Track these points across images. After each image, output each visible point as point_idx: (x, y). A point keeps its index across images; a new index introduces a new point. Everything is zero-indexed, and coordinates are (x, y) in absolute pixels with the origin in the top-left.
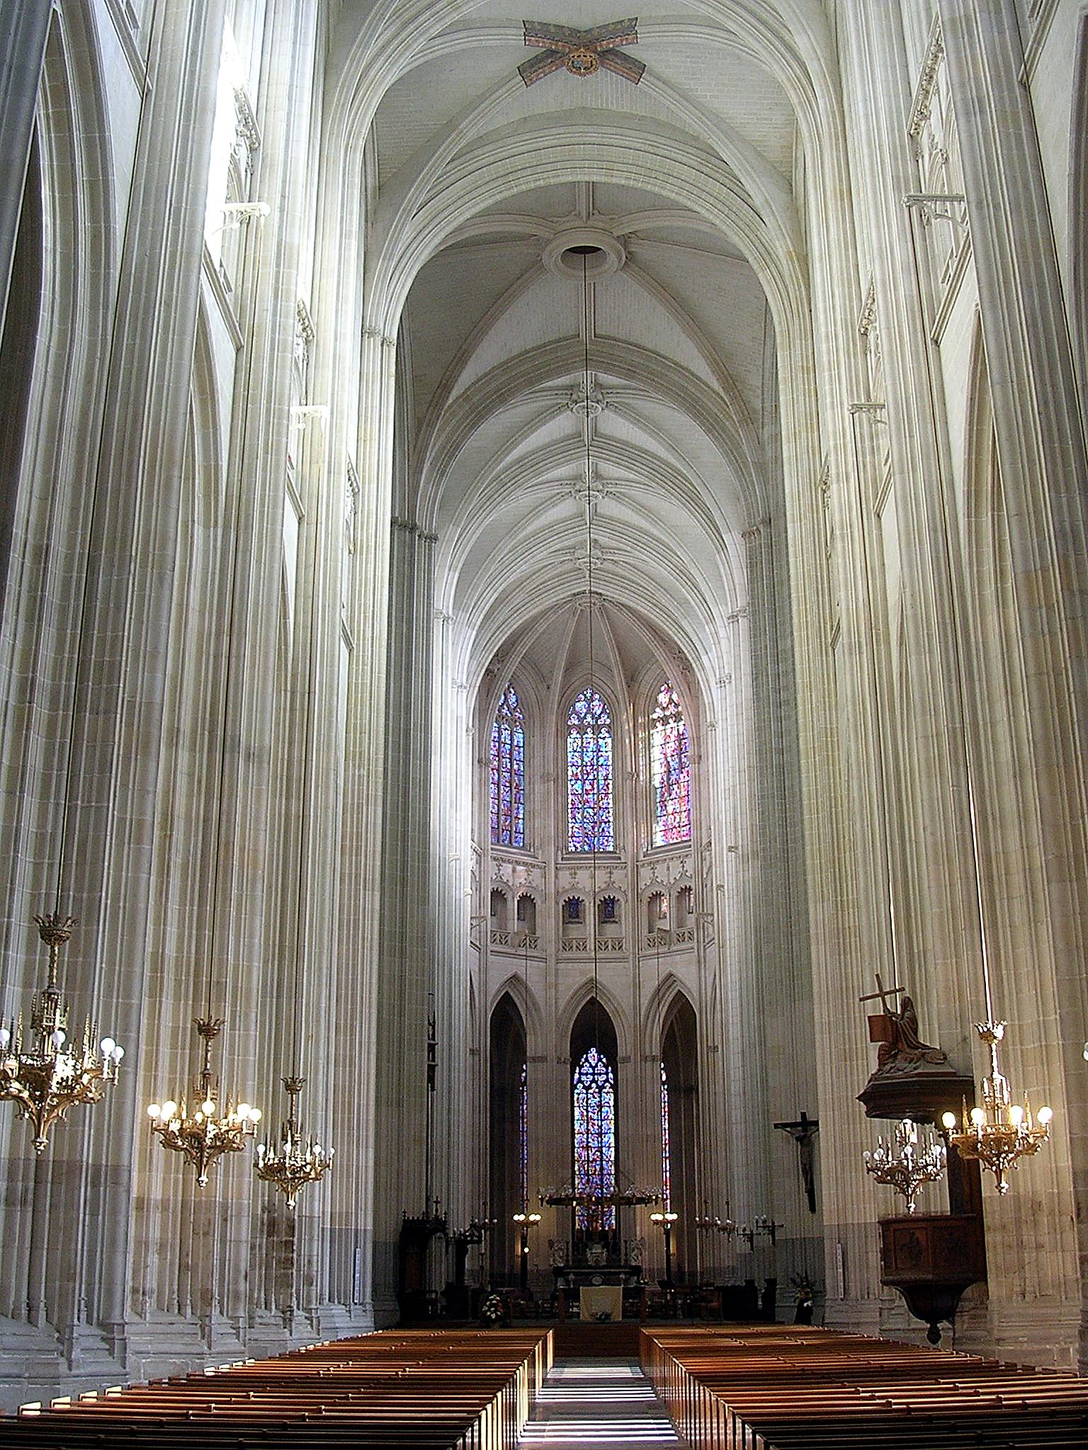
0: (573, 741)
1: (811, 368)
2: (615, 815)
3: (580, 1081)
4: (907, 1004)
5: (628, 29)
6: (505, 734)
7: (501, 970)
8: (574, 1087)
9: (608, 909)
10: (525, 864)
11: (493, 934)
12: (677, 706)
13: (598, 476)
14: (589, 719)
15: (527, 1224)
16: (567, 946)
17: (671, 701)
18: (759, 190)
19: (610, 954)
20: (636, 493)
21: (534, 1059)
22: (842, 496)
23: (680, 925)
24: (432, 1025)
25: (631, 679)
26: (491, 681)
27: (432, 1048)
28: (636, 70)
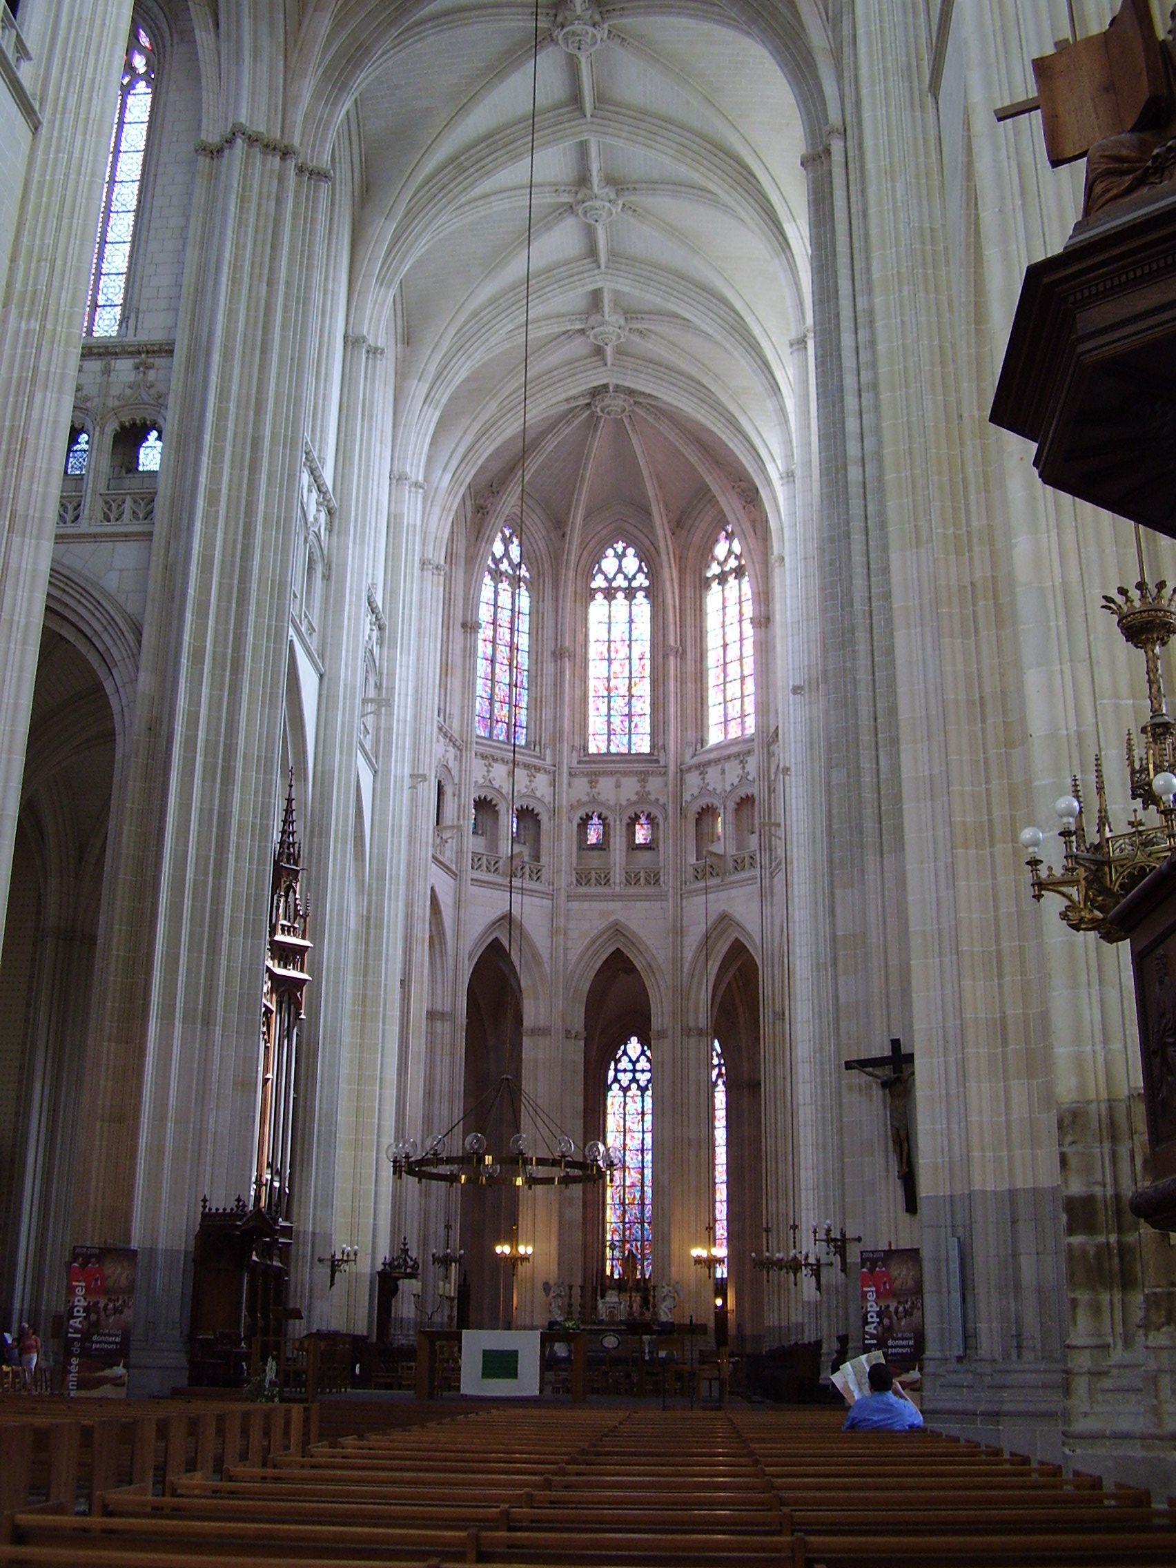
0: (598, 609)
2: (653, 705)
3: (616, 1080)
6: (505, 599)
8: (609, 1088)
10: (527, 766)
11: (477, 857)
12: (737, 557)
15: (514, 1261)
16: (582, 878)
17: (730, 552)
19: (642, 890)
21: (535, 1032)
23: (740, 845)
25: (679, 524)
26: (483, 520)
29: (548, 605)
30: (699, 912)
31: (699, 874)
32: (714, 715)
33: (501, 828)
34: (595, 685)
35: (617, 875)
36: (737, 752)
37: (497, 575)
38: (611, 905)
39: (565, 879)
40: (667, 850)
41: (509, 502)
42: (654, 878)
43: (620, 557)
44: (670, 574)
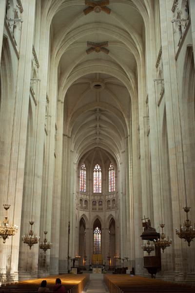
0: (95, 173)
1: (137, 109)
4: (149, 221)
7: (81, 213)
9: (100, 202)
14: (97, 170)
16: (93, 209)
20: (107, 129)
22: (142, 132)
24: (69, 222)
25: (105, 162)
27: (69, 226)
29: (88, 173)
30: (108, 214)
31: (107, 209)
32: (110, 188)
33: (84, 203)
34: (94, 183)
35: (97, 209)
36: (112, 193)
37: (82, 169)
38: (97, 213)
39: (91, 209)
40: (103, 205)
41: (84, 160)
42: (102, 209)
43: (97, 166)
44: (104, 169)
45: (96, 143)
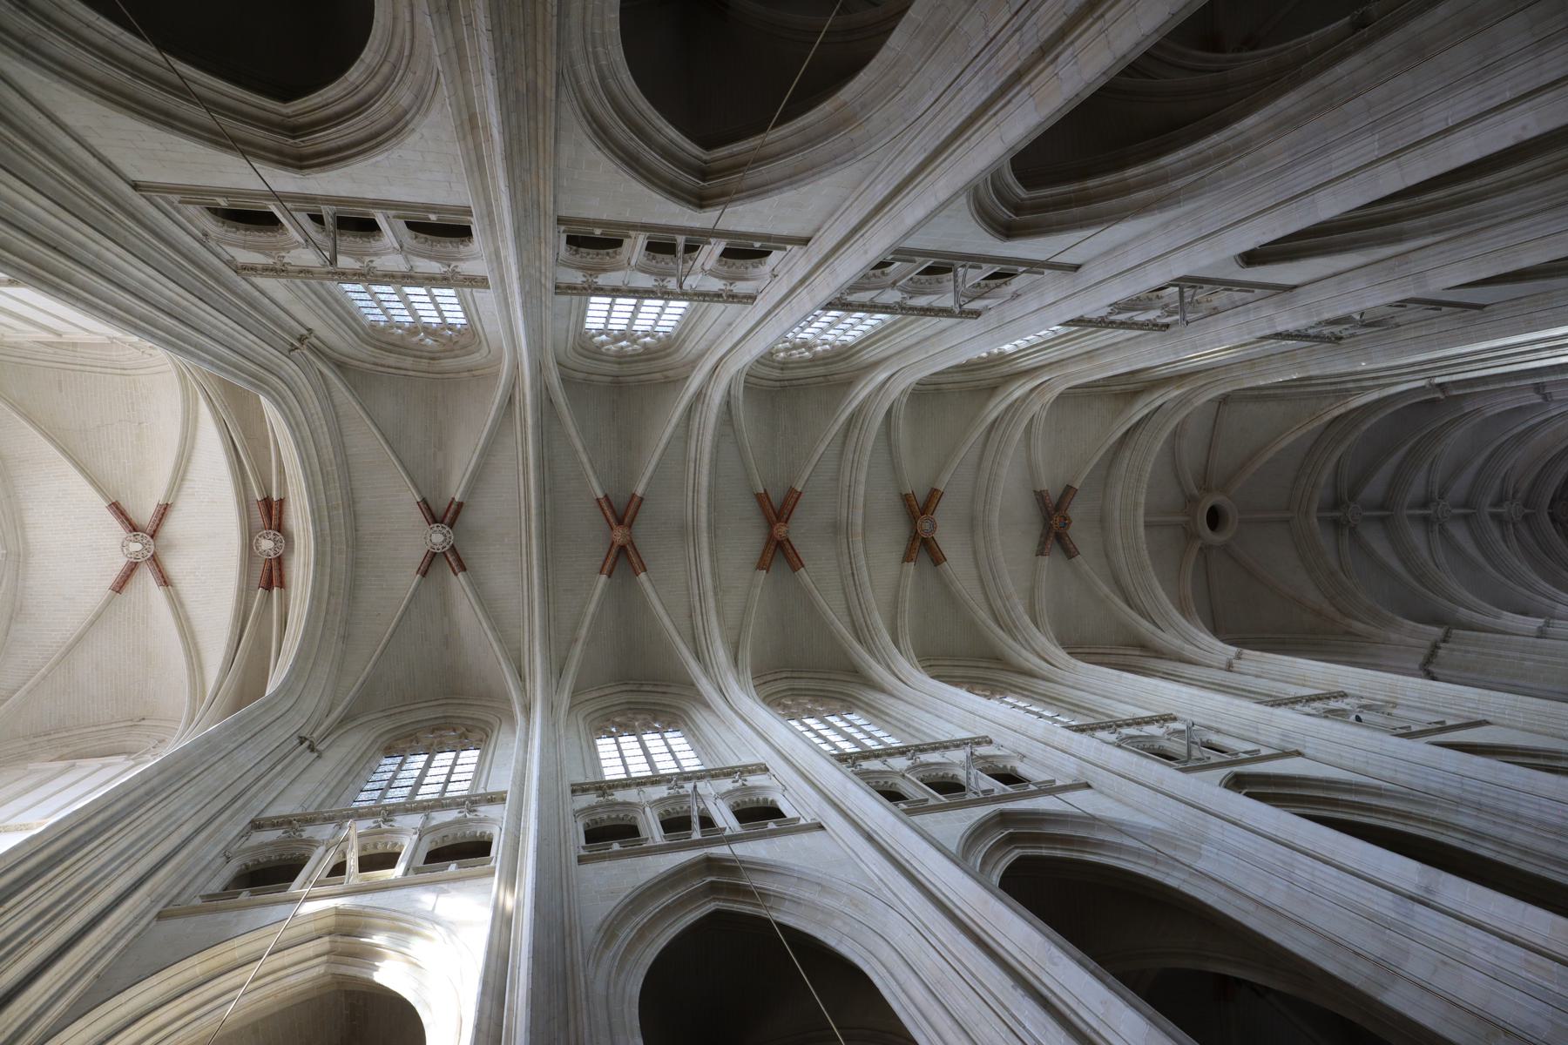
5: (1040, 497)
13: (1425, 504)
18: (1139, 410)
28: (1069, 491)
45: (1526, 518)
